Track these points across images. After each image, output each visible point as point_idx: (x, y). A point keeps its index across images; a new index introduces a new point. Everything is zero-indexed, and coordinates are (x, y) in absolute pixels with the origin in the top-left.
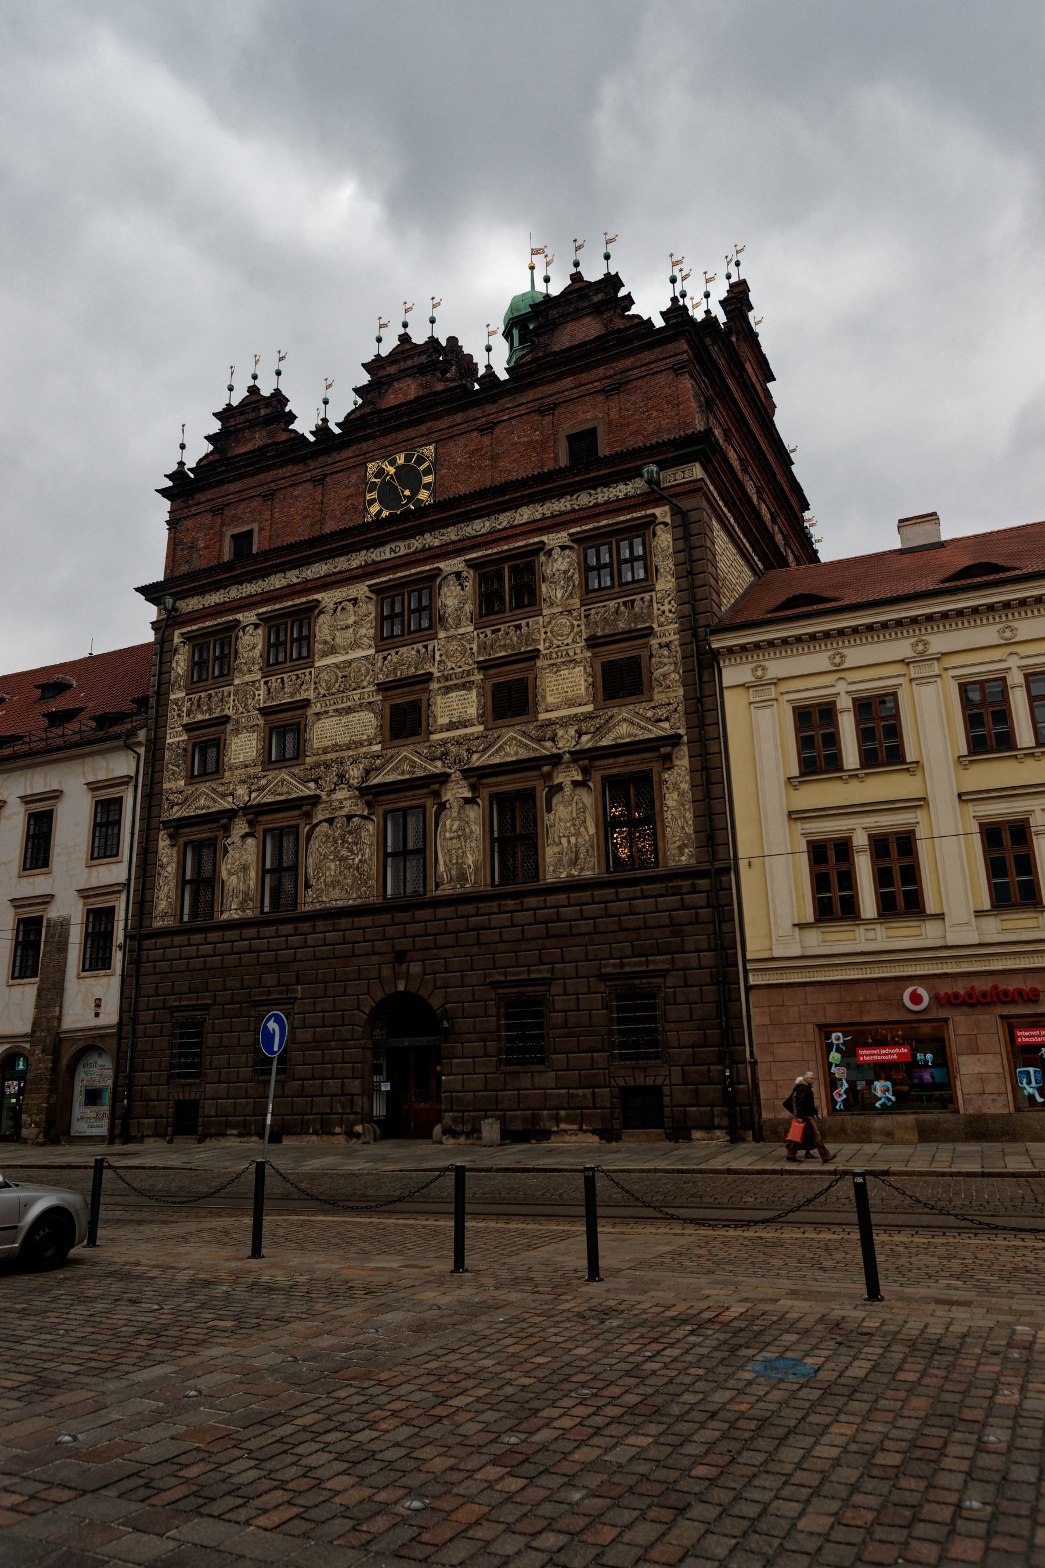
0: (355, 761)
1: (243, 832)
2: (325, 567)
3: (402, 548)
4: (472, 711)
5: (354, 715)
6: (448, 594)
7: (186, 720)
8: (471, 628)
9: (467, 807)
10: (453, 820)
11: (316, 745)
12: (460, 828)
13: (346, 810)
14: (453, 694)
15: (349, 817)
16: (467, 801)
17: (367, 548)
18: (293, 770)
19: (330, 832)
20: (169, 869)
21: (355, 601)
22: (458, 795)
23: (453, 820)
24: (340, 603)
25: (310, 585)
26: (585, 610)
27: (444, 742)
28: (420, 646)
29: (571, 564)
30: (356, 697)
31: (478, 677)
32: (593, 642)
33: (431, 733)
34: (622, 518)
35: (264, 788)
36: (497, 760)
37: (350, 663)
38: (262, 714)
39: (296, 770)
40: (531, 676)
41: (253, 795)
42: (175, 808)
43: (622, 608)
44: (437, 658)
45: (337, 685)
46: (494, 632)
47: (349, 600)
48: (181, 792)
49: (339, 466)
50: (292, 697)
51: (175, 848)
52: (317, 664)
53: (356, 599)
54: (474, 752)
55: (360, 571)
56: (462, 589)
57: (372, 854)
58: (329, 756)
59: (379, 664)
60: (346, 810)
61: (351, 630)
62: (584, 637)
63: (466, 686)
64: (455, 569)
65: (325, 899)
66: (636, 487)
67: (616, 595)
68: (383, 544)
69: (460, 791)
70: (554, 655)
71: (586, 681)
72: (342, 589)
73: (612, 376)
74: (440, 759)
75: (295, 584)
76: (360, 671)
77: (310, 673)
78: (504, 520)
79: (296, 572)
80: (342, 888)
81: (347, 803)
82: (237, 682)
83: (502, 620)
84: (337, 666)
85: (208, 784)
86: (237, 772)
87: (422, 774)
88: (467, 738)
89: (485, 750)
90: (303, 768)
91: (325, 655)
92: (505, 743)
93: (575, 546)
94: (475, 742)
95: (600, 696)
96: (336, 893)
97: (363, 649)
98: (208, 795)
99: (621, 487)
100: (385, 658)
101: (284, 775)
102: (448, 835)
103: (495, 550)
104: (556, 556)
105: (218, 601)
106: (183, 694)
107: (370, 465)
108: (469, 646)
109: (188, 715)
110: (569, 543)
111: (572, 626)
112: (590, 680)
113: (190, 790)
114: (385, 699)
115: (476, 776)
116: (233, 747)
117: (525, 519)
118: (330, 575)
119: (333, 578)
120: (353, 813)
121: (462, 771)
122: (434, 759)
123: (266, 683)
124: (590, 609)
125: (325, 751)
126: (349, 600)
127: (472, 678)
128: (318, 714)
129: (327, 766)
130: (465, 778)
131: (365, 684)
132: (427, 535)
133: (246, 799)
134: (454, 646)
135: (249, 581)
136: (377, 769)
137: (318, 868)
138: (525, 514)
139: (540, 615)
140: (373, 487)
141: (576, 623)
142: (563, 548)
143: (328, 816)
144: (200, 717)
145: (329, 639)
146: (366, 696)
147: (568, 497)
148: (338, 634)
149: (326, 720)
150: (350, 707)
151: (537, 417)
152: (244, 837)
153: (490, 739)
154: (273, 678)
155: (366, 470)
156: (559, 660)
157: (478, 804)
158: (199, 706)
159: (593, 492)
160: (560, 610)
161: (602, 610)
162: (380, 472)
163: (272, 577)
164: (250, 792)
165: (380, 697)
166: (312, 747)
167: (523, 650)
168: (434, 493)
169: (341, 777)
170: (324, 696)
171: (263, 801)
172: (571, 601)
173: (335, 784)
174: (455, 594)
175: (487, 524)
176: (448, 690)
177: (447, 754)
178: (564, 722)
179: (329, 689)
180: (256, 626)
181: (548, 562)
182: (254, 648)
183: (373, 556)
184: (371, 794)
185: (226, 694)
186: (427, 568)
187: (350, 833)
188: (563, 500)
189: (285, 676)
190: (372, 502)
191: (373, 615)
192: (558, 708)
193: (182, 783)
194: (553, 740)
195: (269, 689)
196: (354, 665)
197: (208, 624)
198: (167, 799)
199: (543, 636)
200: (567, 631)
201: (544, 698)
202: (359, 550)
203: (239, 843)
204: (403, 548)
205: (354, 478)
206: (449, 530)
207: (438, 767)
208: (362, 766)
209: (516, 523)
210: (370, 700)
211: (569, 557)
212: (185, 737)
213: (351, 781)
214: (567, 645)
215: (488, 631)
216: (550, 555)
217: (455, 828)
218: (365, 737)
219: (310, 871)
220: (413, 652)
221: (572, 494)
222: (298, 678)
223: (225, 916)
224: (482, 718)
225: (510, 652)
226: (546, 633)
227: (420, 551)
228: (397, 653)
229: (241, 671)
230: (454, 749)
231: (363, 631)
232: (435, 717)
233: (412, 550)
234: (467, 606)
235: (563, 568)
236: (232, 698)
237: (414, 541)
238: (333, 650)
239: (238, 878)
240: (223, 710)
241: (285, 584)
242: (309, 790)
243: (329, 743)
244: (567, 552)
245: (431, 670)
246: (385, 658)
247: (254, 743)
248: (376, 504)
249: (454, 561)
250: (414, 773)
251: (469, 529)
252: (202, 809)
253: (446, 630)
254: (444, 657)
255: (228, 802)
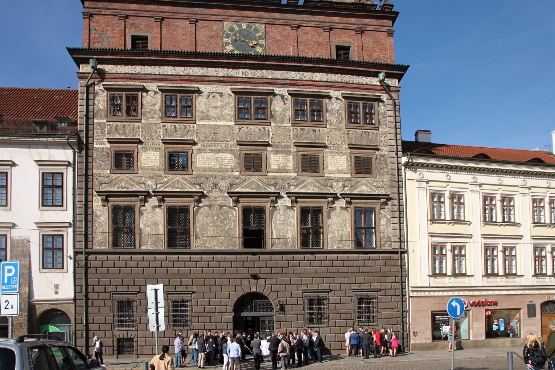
0: (223, 178)
1: (153, 205)
2: (201, 71)
3: (250, 73)
4: (291, 165)
5: (222, 154)
6: (277, 105)
7: (109, 137)
8: (290, 125)
9: (289, 210)
10: (280, 216)
11: (199, 166)
12: (284, 220)
13: (219, 202)
14: (281, 155)
15: (221, 206)
16: (288, 207)
17: (228, 68)
18: (185, 176)
19: (210, 212)
20: (102, 218)
21: (221, 95)
22: (283, 204)
23: (281, 215)
24: (212, 93)
25: (192, 78)
26: (347, 131)
27: (275, 178)
28: (261, 127)
29: (341, 107)
30: (223, 146)
31: (293, 149)
32: (352, 147)
33: (267, 172)
34: (364, 93)
35: (165, 183)
36: (303, 191)
37: (219, 126)
38: (163, 143)
39: (186, 177)
40: (321, 155)
41: (158, 186)
42: (104, 185)
43: (364, 134)
44: (271, 135)
45: (211, 137)
46: (301, 130)
47: (218, 93)
48: (107, 177)
49: (206, 17)
50: (182, 137)
51: (106, 208)
52: (197, 123)
53: (222, 94)
54: (291, 185)
55: (225, 79)
56: (285, 104)
57: (235, 226)
58: (207, 173)
59: (237, 131)
60: (219, 202)
61: (219, 109)
62: (347, 143)
63: (288, 153)
64: (281, 93)
65: (207, 245)
66: (375, 81)
67: (362, 128)
68: (239, 68)
69: (285, 202)
70: (332, 148)
71: (347, 163)
72: (213, 86)
73: (358, 25)
74: (273, 185)
75: (181, 75)
76: (225, 132)
77: (194, 127)
78: (307, 76)
79: (182, 68)
80: (218, 241)
81: (221, 198)
82: (143, 121)
83: (306, 125)
84: (211, 127)
85: (127, 175)
86: (146, 172)
87: (263, 191)
88: (288, 178)
89: (297, 186)
90: (191, 176)
91: (202, 119)
92: (308, 184)
93: (343, 100)
94: (292, 181)
95: (354, 171)
96: (214, 243)
97: (227, 121)
98: (127, 181)
99: (364, 78)
100: (240, 129)
101: (178, 177)
102: (278, 222)
103: (302, 90)
104: (334, 102)
105: (127, 72)
106: (105, 121)
107: (225, 23)
108: (288, 134)
109: (109, 134)
110: (341, 97)
111: (341, 136)
112: (349, 163)
113: (114, 176)
114: (240, 150)
115: (296, 197)
116: (143, 157)
117: (318, 79)
118: (204, 76)
119: (207, 78)
120: (223, 204)
121: (287, 193)
122: (270, 185)
123: (163, 126)
124: (349, 131)
125: (205, 170)
126: (218, 93)
127: (291, 150)
128: (199, 149)
129: (207, 178)
130: (288, 197)
131: (229, 140)
132: (264, 71)
133: (154, 187)
134: (280, 132)
135: (150, 65)
136: (237, 184)
137: (203, 229)
138: (318, 76)
139: (326, 127)
140: (228, 36)
141: (343, 136)
142: (337, 99)
143: (207, 204)
144: (118, 136)
145: (205, 110)
146: (229, 146)
147: (340, 75)
148: (211, 109)
149: (205, 154)
150: (219, 150)
151: (321, 30)
152: (154, 207)
153: (300, 180)
154: (169, 125)
155: (223, 25)
156: (334, 151)
157: (294, 210)
158: (116, 129)
159: (351, 76)
160: (335, 128)
161: (355, 133)
162: (232, 29)
163: (166, 67)
164: (157, 184)
165: (239, 149)
166: (196, 166)
167: (317, 142)
168: (265, 50)
169: (216, 185)
170: (203, 141)
171: (165, 190)
172: (340, 125)
173: (212, 188)
174: (281, 106)
175: (298, 75)
176: (277, 153)
177: (277, 184)
178: (337, 180)
179: (205, 138)
180: (156, 93)
181: (329, 104)
182: (155, 104)
183: (232, 73)
184: (238, 197)
185: (136, 126)
186: (265, 88)
187: (222, 214)
188: (337, 76)
189: (177, 125)
190: (227, 44)
191: (233, 104)
192: (333, 173)
193: (108, 172)
194: (331, 187)
195: (166, 130)
196: (221, 128)
197: (120, 83)
198: (97, 179)
199: (327, 138)
200: (338, 138)
201: (327, 167)
202: (223, 68)
203: (151, 210)
204: (250, 74)
205: (215, 27)
206: (277, 72)
207: (272, 189)
208: (228, 182)
209: (313, 79)
210: (232, 149)
211: (340, 104)
212: (108, 145)
213: (221, 188)
214: (339, 145)
215: (299, 128)
216: (331, 101)
217: (282, 219)
218: (229, 167)
219: (198, 230)
220: (256, 129)
221: (342, 74)
222: (185, 128)
223: (144, 248)
224: (295, 170)
225: (310, 141)
226: (328, 136)
227: (260, 78)
228: (247, 128)
229: (145, 116)
230: (280, 182)
231: (226, 112)
232: (270, 164)
233: (256, 76)
234: (287, 114)
235: (338, 107)
236: (141, 130)
237: (257, 72)
238: (208, 117)
239: (151, 228)
240: (135, 136)
241: (175, 74)
242: (196, 189)
243: (207, 166)
244: (339, 101)
245: (267, 141)
246: (240, 129)
247: (158, 158)
248: (231, 46)
249: (280, 89)
250: (258, 190)
251: (288, 75)
252: (123, 188)
253: (275, 122)
254: (274, 136)
255: (142, 187)
